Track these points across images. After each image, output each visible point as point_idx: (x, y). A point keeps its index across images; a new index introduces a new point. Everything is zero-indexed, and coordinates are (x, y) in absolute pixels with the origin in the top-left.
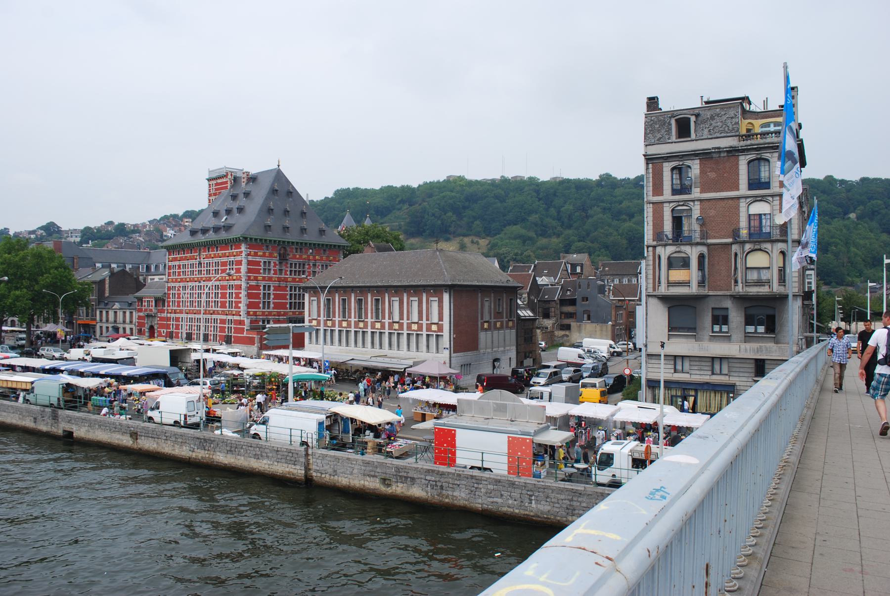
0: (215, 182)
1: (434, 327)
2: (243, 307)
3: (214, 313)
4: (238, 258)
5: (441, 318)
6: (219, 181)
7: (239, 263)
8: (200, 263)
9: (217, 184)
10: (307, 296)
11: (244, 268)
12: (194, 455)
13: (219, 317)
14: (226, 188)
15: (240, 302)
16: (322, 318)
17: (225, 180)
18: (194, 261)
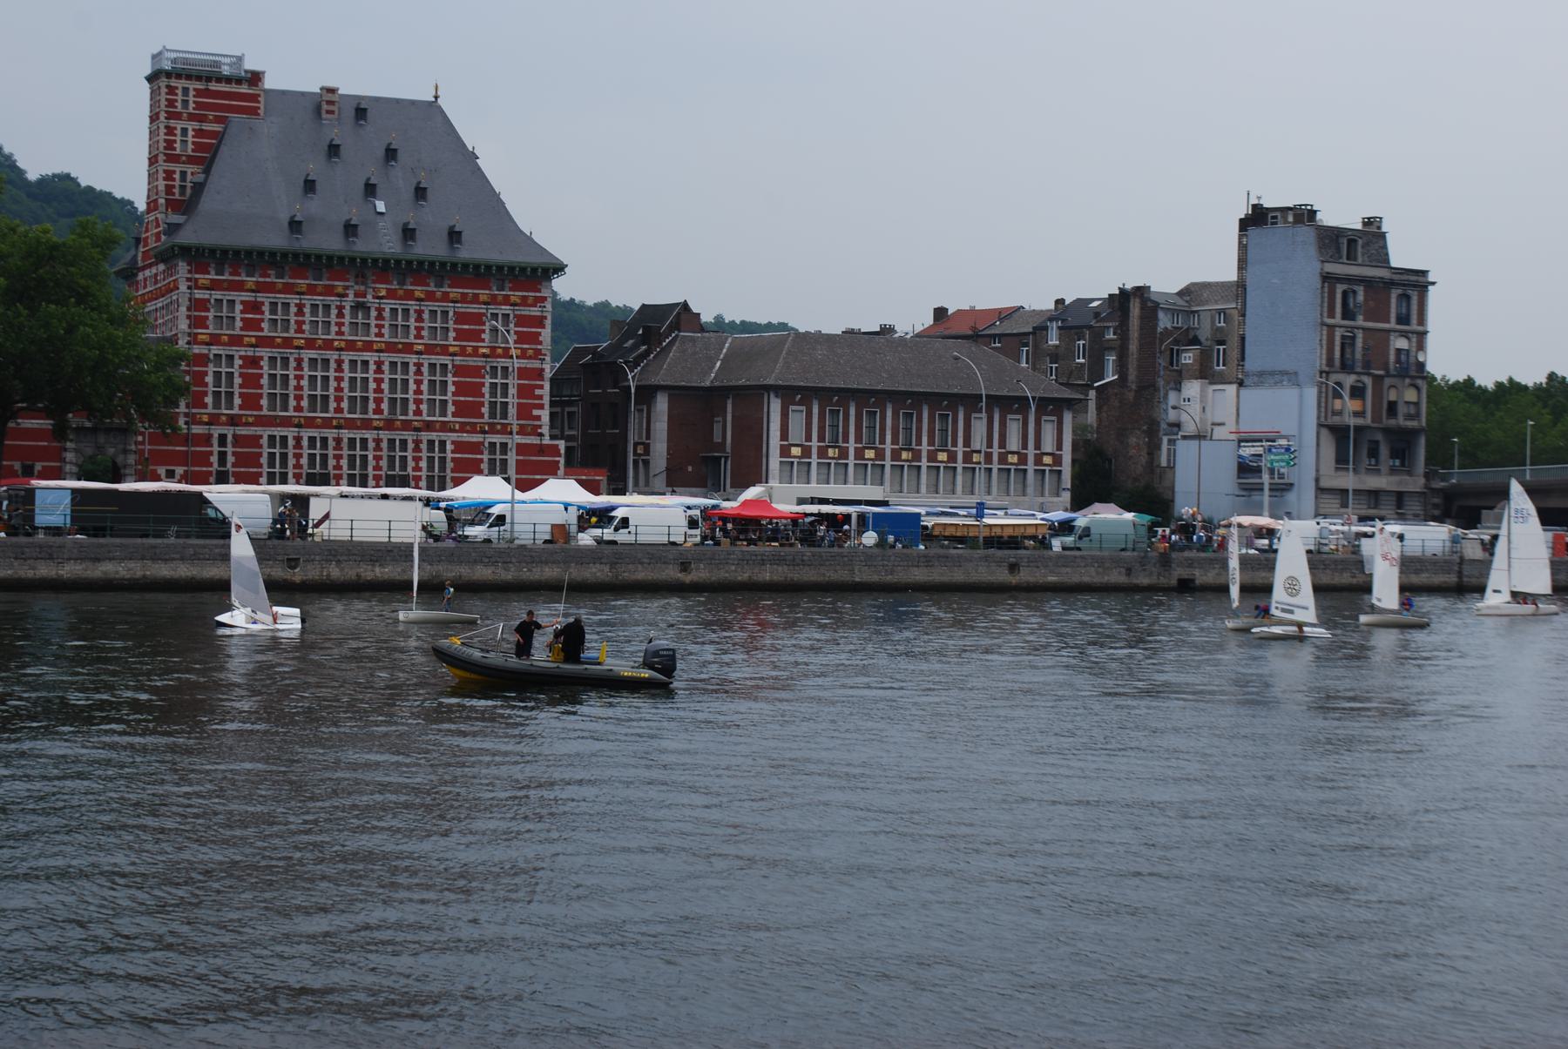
0: (200, 86)
1: (1047, 460)
2: (545, 415)
3: (429, 426)
4: (535, 311)
5: (1060, 447)
6: (214, 86)
7: (540, 321)
8: (359, 307)
9: (199, 93)
10: (776, 406)
11: (546, 334)
12: (1354, 581)
13: (450, 437)
15: (541, 407)
16: (815, 443)
18: (333, 300)
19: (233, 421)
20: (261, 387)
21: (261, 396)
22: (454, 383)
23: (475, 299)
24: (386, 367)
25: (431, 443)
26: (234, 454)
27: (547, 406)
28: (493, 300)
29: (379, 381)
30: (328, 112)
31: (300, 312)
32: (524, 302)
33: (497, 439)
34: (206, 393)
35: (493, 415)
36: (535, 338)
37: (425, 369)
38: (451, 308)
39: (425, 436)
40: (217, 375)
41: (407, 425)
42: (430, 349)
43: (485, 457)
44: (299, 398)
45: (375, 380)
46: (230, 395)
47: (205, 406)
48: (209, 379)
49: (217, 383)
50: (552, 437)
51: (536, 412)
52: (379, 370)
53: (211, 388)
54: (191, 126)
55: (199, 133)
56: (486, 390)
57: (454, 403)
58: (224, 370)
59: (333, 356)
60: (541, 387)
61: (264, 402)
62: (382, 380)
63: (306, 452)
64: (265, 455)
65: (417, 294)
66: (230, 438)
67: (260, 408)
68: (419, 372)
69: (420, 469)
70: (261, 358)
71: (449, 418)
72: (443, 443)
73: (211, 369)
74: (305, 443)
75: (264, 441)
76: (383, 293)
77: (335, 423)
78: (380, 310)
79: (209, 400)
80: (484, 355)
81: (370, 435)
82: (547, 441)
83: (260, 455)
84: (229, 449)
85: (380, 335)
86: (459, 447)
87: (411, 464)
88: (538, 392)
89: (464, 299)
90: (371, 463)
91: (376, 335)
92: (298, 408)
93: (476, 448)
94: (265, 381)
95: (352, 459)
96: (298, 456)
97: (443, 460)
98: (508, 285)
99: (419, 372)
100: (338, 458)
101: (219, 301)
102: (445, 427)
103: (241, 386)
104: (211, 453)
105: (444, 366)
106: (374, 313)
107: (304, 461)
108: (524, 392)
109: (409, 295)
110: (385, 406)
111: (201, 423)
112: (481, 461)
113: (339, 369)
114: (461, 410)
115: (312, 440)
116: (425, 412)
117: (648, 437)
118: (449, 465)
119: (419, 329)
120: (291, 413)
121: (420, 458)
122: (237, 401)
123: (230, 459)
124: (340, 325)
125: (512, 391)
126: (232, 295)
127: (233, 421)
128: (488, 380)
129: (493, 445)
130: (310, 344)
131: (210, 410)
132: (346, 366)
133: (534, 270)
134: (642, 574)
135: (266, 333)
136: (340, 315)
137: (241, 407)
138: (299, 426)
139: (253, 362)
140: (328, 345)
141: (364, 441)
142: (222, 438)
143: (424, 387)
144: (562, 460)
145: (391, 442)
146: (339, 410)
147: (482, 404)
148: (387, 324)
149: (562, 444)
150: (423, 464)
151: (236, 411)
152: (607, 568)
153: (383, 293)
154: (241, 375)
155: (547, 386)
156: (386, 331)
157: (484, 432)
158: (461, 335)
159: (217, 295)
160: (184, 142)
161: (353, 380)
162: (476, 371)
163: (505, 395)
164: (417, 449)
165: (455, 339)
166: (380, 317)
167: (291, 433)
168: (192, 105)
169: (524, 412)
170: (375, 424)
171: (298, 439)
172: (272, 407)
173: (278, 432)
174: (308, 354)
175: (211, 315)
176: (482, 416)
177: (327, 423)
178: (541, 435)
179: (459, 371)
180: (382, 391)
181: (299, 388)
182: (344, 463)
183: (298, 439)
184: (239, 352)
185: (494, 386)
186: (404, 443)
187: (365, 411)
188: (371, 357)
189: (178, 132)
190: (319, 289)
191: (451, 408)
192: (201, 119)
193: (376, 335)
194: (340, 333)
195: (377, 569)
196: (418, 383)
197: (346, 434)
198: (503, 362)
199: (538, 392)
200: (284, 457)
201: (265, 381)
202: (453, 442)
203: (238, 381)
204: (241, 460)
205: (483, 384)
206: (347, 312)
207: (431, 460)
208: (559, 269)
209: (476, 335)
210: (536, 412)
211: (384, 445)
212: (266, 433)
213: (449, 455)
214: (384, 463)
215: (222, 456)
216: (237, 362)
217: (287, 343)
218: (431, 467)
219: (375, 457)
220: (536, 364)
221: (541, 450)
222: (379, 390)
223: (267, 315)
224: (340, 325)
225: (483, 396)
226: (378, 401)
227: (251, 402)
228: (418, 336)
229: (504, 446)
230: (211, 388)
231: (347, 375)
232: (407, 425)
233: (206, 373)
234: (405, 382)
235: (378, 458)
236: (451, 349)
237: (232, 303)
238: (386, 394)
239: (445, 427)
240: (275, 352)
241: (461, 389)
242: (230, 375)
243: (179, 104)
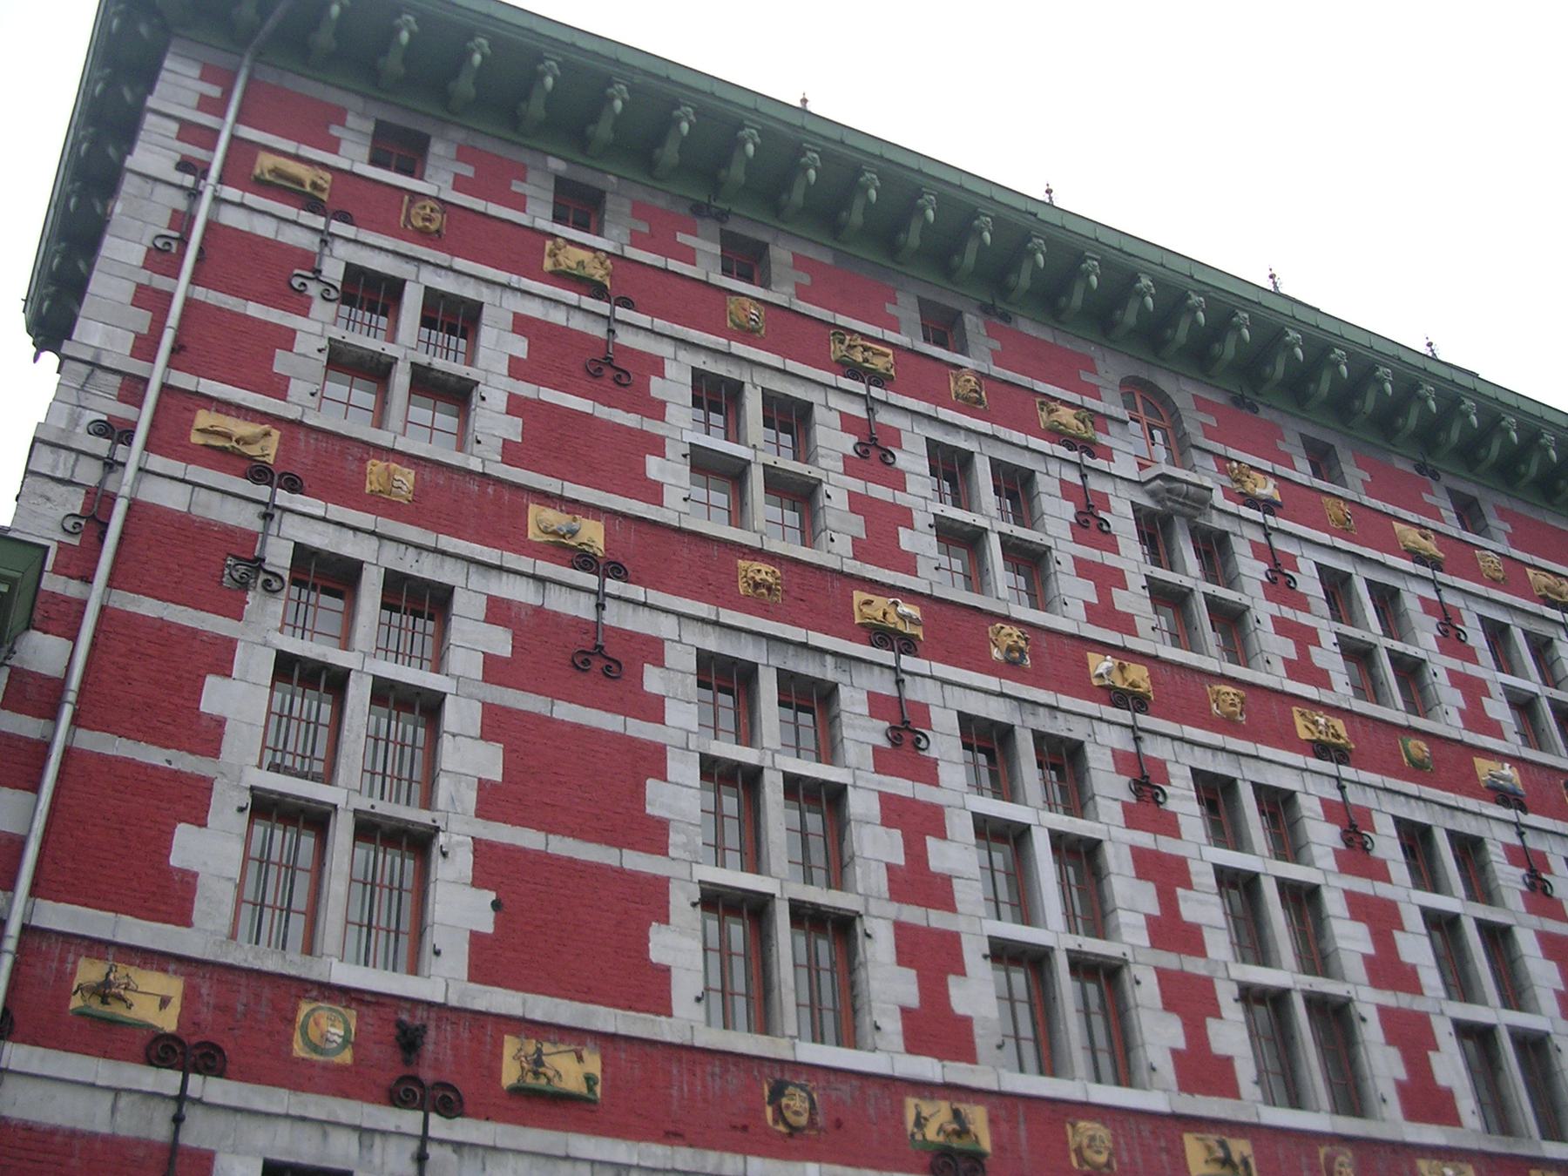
34: (193, 800)
44: (931, 956)
47: (172, 897)
70: (653, 650)
73: (264, 630)
79: (210, 850)
103: (491, 801)
111: (106, 1035)
120: (887, 1057)
122: (460, 907)
131: (207, 934)
137: (488, 960)
151: (443, 980)
184: (478, 582)
201: (678, 796)
203: (470, 759)
216: (474, 638)
217: (812, 593)
227: (567, 928)
230: (242, 766)
233: (220, 656)
240: (747, 636)
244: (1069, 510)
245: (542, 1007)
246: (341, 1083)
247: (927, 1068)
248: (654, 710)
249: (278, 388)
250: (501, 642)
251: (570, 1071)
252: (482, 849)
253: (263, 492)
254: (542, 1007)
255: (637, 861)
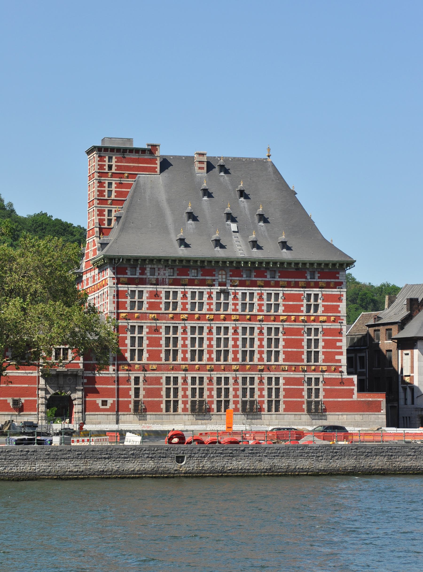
2: (343, 359)
3: (269, 368)
13: (282, 375)
14: (153, 170)
15: (341, 354)
17: (147, 156)
19: (144, 368)
20: (161, 346)
21: (160, 351)
22: (284, 340)
23: (296, 285)
24: (240, 331)
25: (270, 379)
26: (144, 389)
27: (345, 353)
28: (308, 285)
29: (235, 340)
30: (200, 168)
31: (184, 296)
32: (328, 286)
33: (313, 375)
35: (309, 360)
36: (336, 309)
37: (265, 331)
38: (281, 291)
39: (266, 375)
40: (133, 339)
41: (253, 368)
42: (267, 318)
43: (305, 387)
45: (233, 339)
46: (141, 352)
48: (128, 342)
49: (133, 344)
50: (349, 373)
51: (337, 357)
52: (236, 332)
53: (129, 348)
54: (114, 181)
55: (120, 185)
56: (305, 344)
57: (284, 352)
58: (136, 335)
59: (206, 325)
60: (341, 341)
61: (163, 355)
62: (237, 339)
63: (190, 387)
64: (164, 389)
65: (259, 283)
66: (141, 380)
67: (160, 359)
68: (261, 333)
69: (263, 396)
70: (161, 327)
71: (281, 362)
72: (277, 379)
74: (189, 381)
75: (163, 381)
76: (237, 283)
77: (208, 367)
78: (235, 294)
80: (303, 321)
81: (231, 375)
82: (345, 376)
83: (161, 389)
84: (141, 386)
85: (235, 310)
86: (288, 381)
87: (257, 393)
88: (338, 344)
89: (289, 285)
90: (232, 393)
91: (233, 310)
92: (184, 359)
93: (299, 381)
94: (163, 342)
95: (219, 390)
96: (185, 390)
97: (278, 390)
98: (317, 275)
99: (261, 333)
100: (210, 390)
101: (133, 292)
102: (278, 368)
103: (148, 346)
104: (130, 389)
105: (277, 329)
106: (231, 297)
107: (189, 393)
108: (328, 344)
109: (254, 284)
110: (240, 356)
112: (303, 390)
113: (210, 332)
114: (289, 357)
115: (194, 379)
116: (265, 359)
117: (412, 371)
118: (282, 393)
119: (260, 305)
121: (263, 389)
123: (142, 393)
124: (210, 304)
125: (321, 344)
126: (141, 287)
127: (144, 368)
128: (306, 337)
129: (310, 379)
130: (191, 317)
132: (214, 331)
133: (334, 265)
134: (409, 463)
135: (163, 311)
136: (210, 298)
137: (148, 359)
138: (186, 370)
139: (157, 330)
140: (201, 317)
141: (227, 379)
142: (137, 380)
143: (265, 343)
144: (355, 388)
145: (244, 379)
146: (210, 359)
147: (302, 353)
148: (240, 302)
149: (355, 378)
150: (265, 393)
152: (385, 459)
153: (237, 283)
154: (148, 338)
155: (344, 339)
156: (239, 307)
157: (304, 371)
158: (287, 308)
159: (132, 287)
160: (110, 192)
161: (219, 340)
162: (298, 332)
163: (316, 346)
164: (261, 382)
165: (284, 311)
166: (235, 298)
167: (180, 375)
168: (114, 168)
169: (329, 357)
170: (234, 367)
171: (185, 379)
172: (167, 359)
173: (172, 374)
174: (189, 324)
175: (128, 300)
176: (302, 360)
177: (202, 368)
178: (341, 372)
179: (286, 332)
180: (237, 346)
181: (184, 345)
182: (214, 393)
183: (185, 379)
184: (146, 324)
185: (309, 341)
186: (252, 380)
187: (226, 359)
188: (230, 324)
189: (106, 185)
190: (196, 282)
191: (282, 356)
192: (121, 175)
193: (233, 310)
194: (210, 309)
195: (234, 463)
196: (261, 340)
197: (215, 375)
198: (314, 325)
199: (338, 344)
200: (176, 390)
202: (284, 378)
204: (149, 393)
205: (303, 340)
206: (214, 296)
207: (270, 390)
208: (350, 263)
209: (298, 309)
210: (337, 357)
211: (240, 381)
212: (164, 375)
213: (281, 386)
214: (240, 393)
215: (137, 390)
216: (145, 330)
217: (176, 316)
218: (270, 395)
219: (234, 389)
220: (336, 326)
221: (342, 382)
222: (235, 346)
223: (164, 300)
224: (210, 304)
225: (303, 347)
226: (235, 353)
228: (260, 310)
229: (317, 379)
231: (215, 336)
232: (253, 368)
233: (126, 338)
234: (252, 340)
235: (236, 390)
236: (281, 318)
237: (141, 292)
238: (240, 349)
239: (278, 368)
241: (288, 343)
242: (141, 339)
243: (106, 167)
244: (207, 296)
245: (152, 362)
246: (138, 370)
247: (183, 362)
248: (161, 333)
249: (126, 309)
250: (148, 330)
251: (155, 367)
252: (148, 350)
253: (127, 321)
254: (152, 362)
255: (160, 348)
